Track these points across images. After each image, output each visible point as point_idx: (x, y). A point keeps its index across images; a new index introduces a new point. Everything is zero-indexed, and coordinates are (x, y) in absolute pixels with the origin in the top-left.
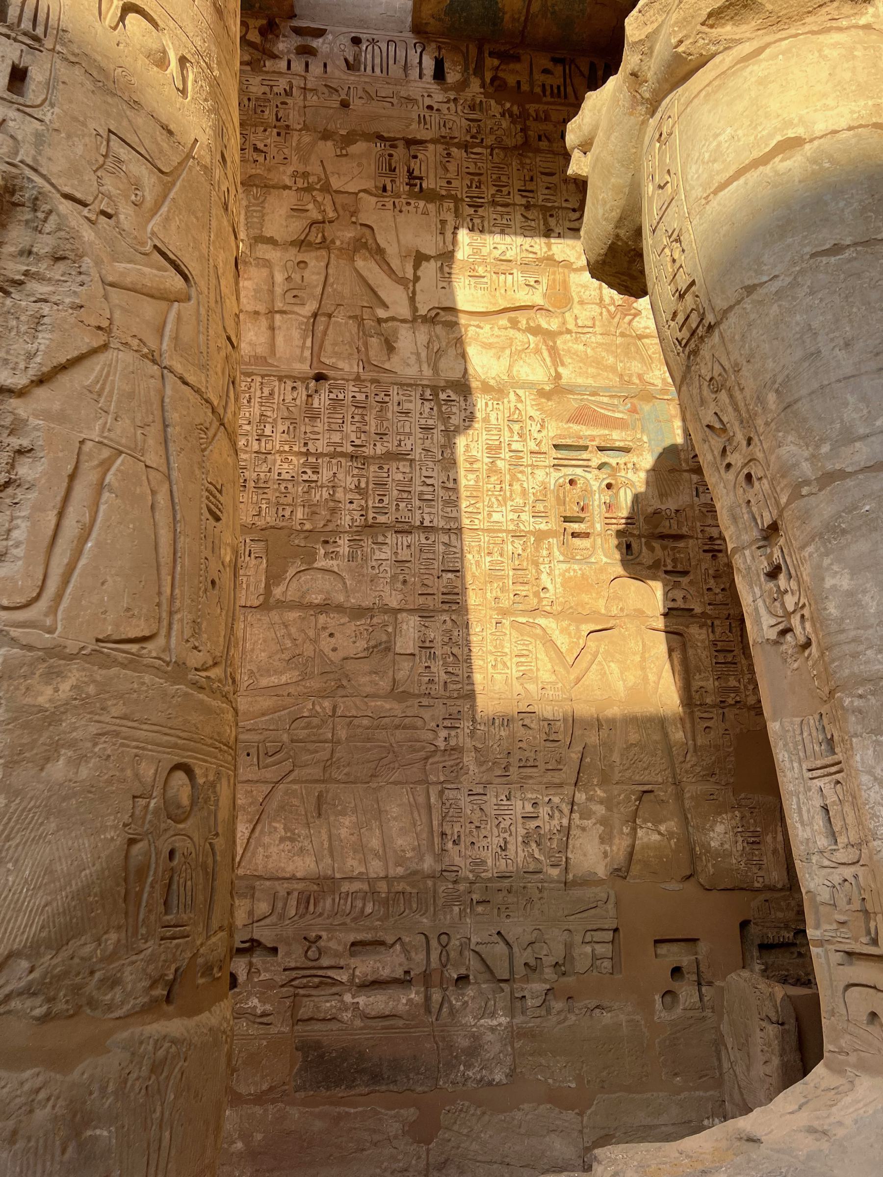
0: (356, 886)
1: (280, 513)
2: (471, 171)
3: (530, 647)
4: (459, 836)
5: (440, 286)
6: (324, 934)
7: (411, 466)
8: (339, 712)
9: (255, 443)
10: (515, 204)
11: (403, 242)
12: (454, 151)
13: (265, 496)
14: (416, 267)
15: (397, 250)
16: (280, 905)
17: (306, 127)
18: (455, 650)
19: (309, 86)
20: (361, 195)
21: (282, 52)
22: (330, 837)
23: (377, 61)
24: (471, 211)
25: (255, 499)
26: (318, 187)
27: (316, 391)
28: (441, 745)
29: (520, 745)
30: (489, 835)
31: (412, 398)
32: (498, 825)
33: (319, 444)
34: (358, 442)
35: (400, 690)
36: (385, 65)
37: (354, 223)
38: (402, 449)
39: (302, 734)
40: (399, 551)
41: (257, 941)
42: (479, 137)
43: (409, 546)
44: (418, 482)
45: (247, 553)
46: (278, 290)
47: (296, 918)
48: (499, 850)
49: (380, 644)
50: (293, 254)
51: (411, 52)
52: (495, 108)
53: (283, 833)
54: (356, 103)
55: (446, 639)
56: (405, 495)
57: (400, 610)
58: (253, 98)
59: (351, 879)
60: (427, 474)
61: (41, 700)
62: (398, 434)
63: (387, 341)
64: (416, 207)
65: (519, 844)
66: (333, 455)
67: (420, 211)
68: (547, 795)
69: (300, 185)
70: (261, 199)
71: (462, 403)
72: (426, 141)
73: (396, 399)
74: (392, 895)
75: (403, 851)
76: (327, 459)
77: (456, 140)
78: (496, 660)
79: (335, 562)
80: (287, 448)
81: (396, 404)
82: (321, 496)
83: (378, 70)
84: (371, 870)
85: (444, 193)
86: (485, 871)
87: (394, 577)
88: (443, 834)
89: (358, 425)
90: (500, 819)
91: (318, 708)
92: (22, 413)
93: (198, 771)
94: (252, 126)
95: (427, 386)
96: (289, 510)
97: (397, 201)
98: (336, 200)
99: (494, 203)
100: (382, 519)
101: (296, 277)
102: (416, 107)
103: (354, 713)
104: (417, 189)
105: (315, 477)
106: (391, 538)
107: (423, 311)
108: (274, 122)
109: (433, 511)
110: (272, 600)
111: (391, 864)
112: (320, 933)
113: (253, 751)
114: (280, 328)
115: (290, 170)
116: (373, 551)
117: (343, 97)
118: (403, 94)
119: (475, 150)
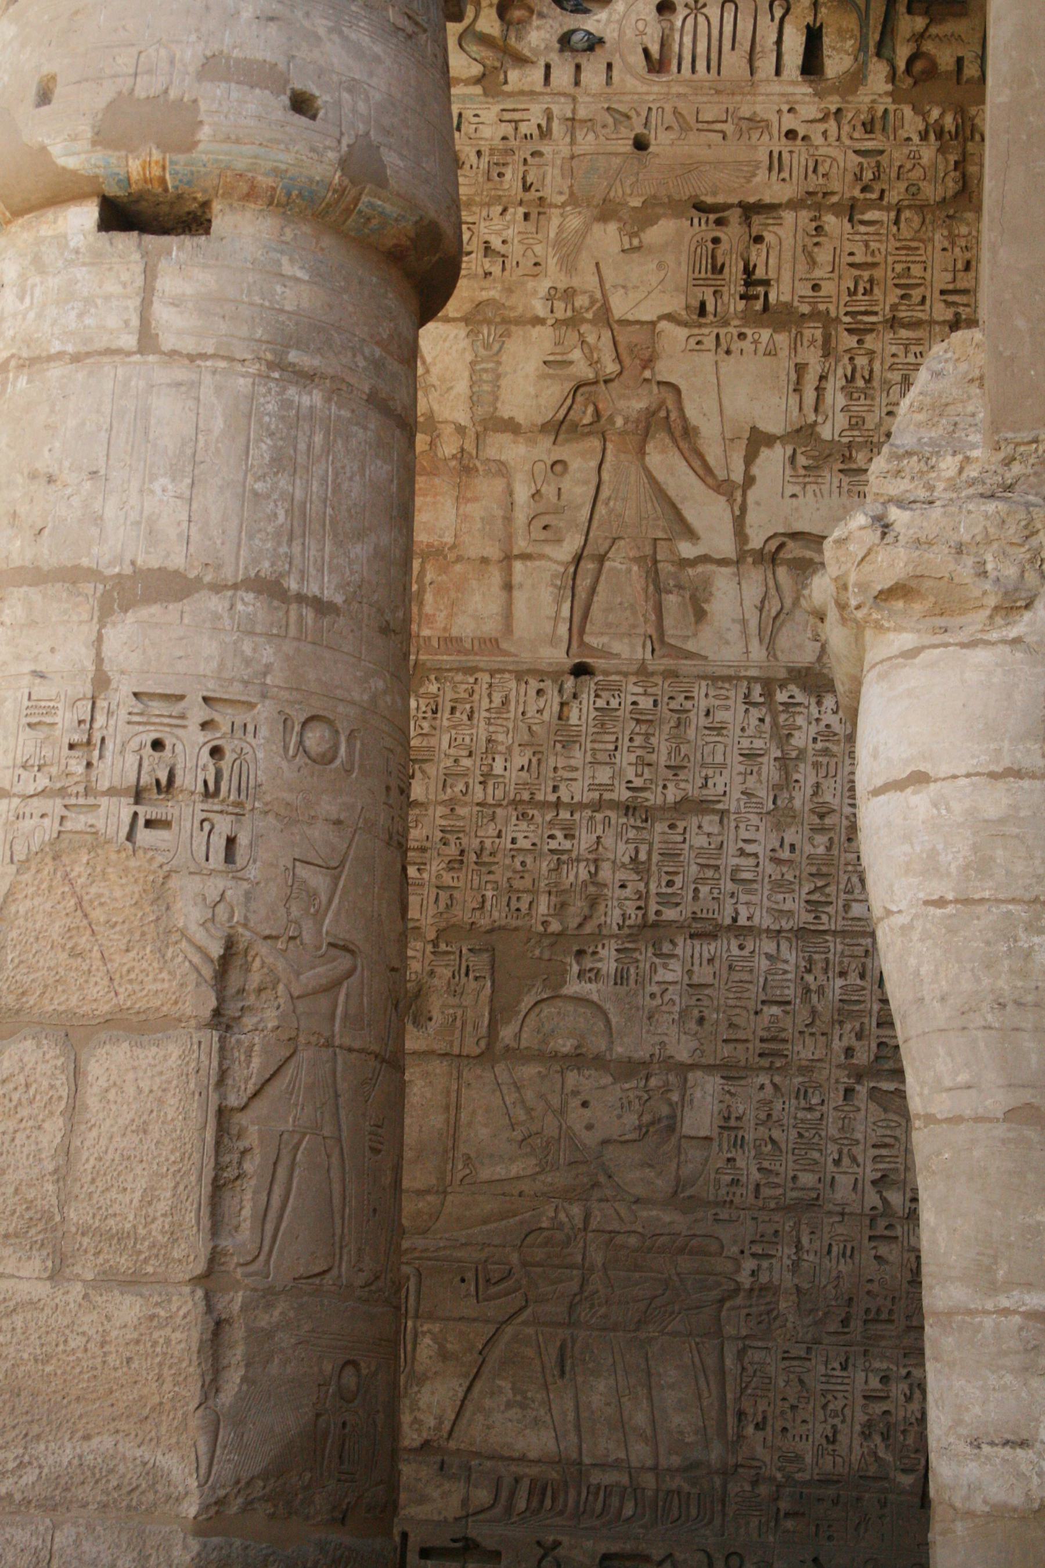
0: (609, 1478)
1: (514, 904)
2: (858, 259)
3: (898, 1133)
4: (764, 1418)
5: (788, 493)
6: (565, 1540)
7: (721, 822)
8: (593, 1225)
9: (479, 788)
10: (932, 322)
11: (729, 411)
12: (830, 221)
13: (491, 877)
14: (750, 459)
15: (718, 429)
16: (504, 1494)
17: (573, 200)
18: (776, 1134)
19: (582, 113)
20: (663, 325)
21: (535, 51)
22: (577, 1407)
23: (702, 48)
24: (851, 341)
25: (476, 882)
26: (589, 315)
27: (575, 696)
28: (745, 1279)
29: (869, 1286)
30: (810, 1419)
31: (730, 702)
32: (824, 1407)
33: (576, 787)
34: (638, 782)
35: (687, 1194)
36: (714, 56)
37: (646, 380)
38: (710, 793)
39: (539, 1254)
40: (696, 968)
41: (473, 1541)
42: (877, 187)
43: (710, 961)
44: (731, 848)
45: (463, 970)
46: (521, 517)
47: (528, 1514)
48: (824, 1441)
49: (660, 1120)
50: (544, 449)
51: (764, 20)
52: (911, 123)
53: (510, 1394)
54: (661, 142)
55: (763, 1116)
56: (710, 873)
57: (693, 1067)
58: (486, 151)
59: (603, 1466)
60: (747, 836)
61: (263, 1324)
62: (703, 765)
63: (694, 599)
64: (756, 342)
65: (855, 1436)
66: (598, 806)
67: (761, 348)
68: (905, 1366)
69: (560, 314)
70: (496, 347)
71: (814, 710)
72: (780, 205)
73: (704, 704)
74: (661, 1495)
75: (681, 1433)
76: (587, 813)
77: (835, 199)
78: (840, 1153)
79: (593, 986)
80: (526, 796)
81: (702, 713)
82: (576, 876)
83: (701, 65)
84: (633, 1458)
85: (805, 309)
86: (800, 1470)
87: (684, 1013)
88: (741, 1415)
89: (640, 752)
90: (829, 1397)
91: (562, 1216)
92: (244, 1122)
93: (363, 1364)
94: (482, 205)
95: (756, 679)
96: (526, 898)
97: (722, 331)
98: (619, 338)
99: (893, 323)
100: (670, 914)
101: (549, 491)
102: (766, 137)
103: (615, 1226)
104: (759, 305)
105: (567, 845)
106: (683, 947)
107: (756, 542)
108: (521, 194)
109: (754, 899)
110: (499, 1046)
111: (662, 1450)
112: (559, 1538)
113: (470, 1275)
114: (521, 586)
115: (544, 286)
116: (654, 968)
117: (639, 129)
118: (745, 111)
119: (868, 216)
